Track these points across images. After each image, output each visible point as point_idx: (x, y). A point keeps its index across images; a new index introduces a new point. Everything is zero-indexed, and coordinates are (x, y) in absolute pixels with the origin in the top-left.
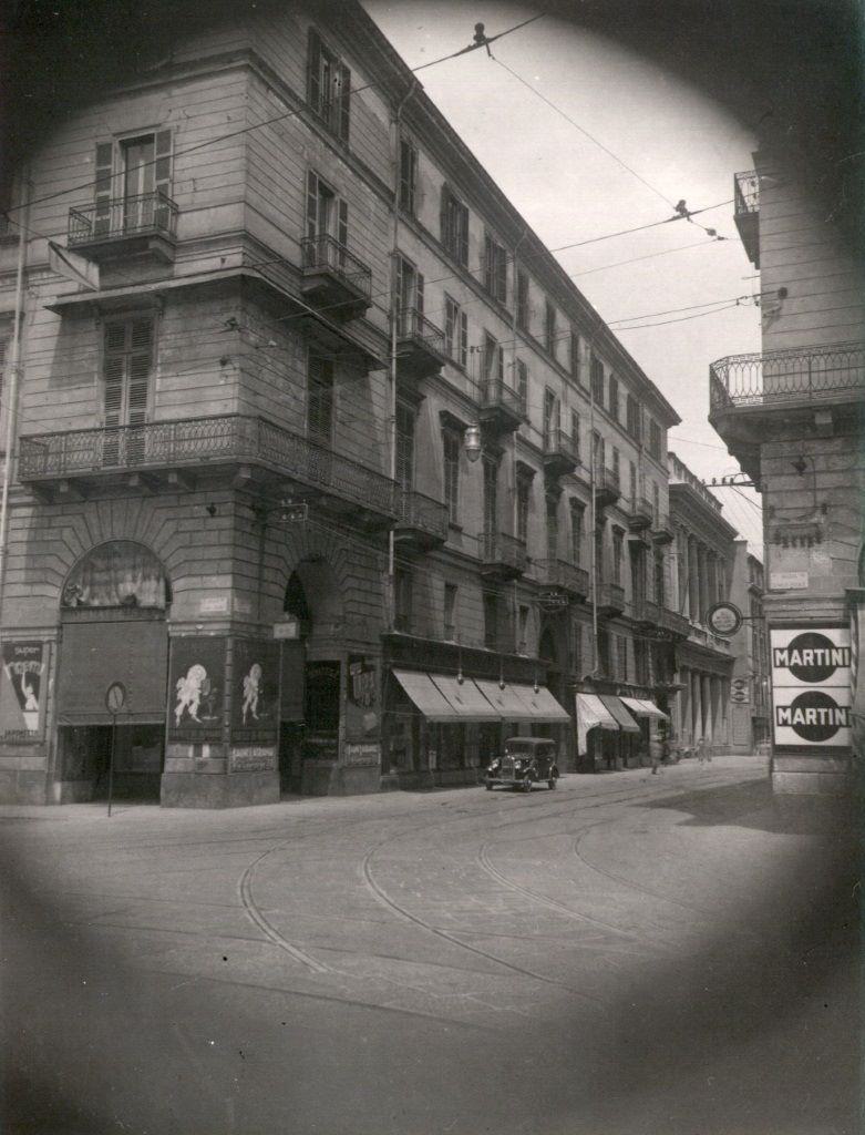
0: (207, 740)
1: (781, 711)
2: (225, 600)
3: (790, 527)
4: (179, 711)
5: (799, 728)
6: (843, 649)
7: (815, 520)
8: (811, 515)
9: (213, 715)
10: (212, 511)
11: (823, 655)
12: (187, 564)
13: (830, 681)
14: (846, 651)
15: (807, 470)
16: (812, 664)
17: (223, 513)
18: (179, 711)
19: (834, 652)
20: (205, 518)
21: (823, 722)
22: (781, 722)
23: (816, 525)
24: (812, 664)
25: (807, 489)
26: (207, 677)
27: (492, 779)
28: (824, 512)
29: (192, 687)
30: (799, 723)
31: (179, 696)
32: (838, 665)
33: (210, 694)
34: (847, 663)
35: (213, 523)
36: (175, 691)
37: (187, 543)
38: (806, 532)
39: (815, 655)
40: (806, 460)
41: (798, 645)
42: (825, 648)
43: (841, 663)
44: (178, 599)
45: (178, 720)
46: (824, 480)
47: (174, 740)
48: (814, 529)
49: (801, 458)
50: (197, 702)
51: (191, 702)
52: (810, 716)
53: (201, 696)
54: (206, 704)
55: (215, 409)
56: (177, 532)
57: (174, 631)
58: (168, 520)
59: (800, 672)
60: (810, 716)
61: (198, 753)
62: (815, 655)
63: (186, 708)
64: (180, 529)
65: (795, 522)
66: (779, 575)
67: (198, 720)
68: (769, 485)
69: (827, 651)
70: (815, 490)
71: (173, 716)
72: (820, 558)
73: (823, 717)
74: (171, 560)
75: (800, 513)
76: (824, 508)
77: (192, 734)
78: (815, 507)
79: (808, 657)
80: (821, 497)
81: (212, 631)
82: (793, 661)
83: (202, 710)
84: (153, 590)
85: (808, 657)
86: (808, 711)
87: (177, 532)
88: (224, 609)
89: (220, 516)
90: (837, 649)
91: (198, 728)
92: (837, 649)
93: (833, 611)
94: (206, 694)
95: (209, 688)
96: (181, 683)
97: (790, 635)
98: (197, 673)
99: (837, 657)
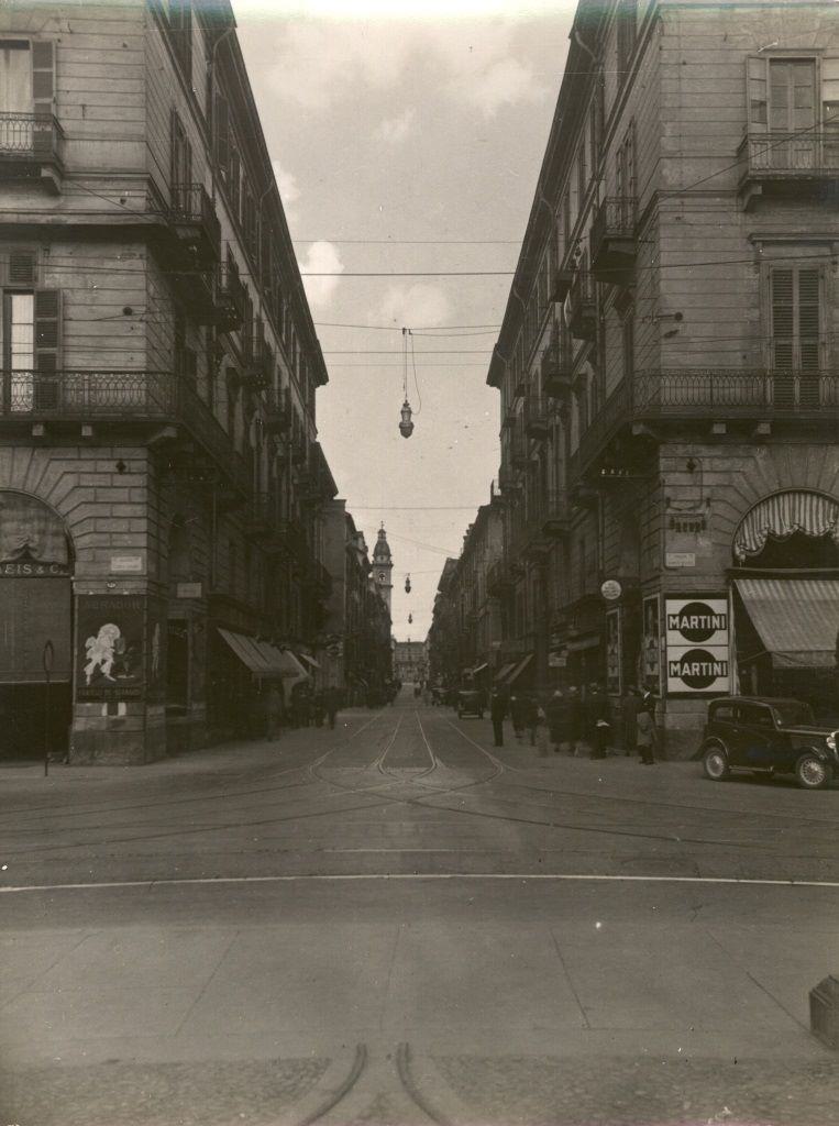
0: (125, 699)
1: (673, 665)
2: (140, 559)
3: (681, 515)
4: (89, 670)
5: (686, 679)
7: (700, 511)
8: (698, 507)
9: (128, 674)
10: (121, 469)
12: (92, 521)
14: (723, 618)
15: (696, 469)
17: (135, 471)
18: (89, 670)
20: (112, 474)
21: (704, 674)
25: (695, 485)
28: (708, 505)
29: (102, 648)
32: (716, 629)
33: (126, 652)
35: (120, 480)
36: (83, 650)
37: (91, 498)
38: (693, 521)
40: (695, 461)
41: (686, 612)
42: (707, 615)
44: (82, 556)
45: (88, 680)
46: (708, 479)
47: (83, 699)
49: (691, 459)
50: (110, 661)
51: (104, 661)
53: (115, 655)
56: (78, 487)
57: (79, 589)
58: (66, 473)
59: (686, 633)
61: (113, 710)
63: (97, 667)
64: (83, 483)
66: (672, 555)
71: (82, 675)
72: (704, 542)
75: (692, 505)
77: (101, 691)
78: (701, 500)
79: (693, 622)
80: (706, 492)
81: (126, 589)
83: (115, 670)
85: (693, 622)
87: (78, 487)
88: (139, 568)
89: (130, 473)
91: (112, 686)
92: (716, 616)
94: (121, 652)
96: (90, 642)
97: (684, 603)
98: (108, 635)
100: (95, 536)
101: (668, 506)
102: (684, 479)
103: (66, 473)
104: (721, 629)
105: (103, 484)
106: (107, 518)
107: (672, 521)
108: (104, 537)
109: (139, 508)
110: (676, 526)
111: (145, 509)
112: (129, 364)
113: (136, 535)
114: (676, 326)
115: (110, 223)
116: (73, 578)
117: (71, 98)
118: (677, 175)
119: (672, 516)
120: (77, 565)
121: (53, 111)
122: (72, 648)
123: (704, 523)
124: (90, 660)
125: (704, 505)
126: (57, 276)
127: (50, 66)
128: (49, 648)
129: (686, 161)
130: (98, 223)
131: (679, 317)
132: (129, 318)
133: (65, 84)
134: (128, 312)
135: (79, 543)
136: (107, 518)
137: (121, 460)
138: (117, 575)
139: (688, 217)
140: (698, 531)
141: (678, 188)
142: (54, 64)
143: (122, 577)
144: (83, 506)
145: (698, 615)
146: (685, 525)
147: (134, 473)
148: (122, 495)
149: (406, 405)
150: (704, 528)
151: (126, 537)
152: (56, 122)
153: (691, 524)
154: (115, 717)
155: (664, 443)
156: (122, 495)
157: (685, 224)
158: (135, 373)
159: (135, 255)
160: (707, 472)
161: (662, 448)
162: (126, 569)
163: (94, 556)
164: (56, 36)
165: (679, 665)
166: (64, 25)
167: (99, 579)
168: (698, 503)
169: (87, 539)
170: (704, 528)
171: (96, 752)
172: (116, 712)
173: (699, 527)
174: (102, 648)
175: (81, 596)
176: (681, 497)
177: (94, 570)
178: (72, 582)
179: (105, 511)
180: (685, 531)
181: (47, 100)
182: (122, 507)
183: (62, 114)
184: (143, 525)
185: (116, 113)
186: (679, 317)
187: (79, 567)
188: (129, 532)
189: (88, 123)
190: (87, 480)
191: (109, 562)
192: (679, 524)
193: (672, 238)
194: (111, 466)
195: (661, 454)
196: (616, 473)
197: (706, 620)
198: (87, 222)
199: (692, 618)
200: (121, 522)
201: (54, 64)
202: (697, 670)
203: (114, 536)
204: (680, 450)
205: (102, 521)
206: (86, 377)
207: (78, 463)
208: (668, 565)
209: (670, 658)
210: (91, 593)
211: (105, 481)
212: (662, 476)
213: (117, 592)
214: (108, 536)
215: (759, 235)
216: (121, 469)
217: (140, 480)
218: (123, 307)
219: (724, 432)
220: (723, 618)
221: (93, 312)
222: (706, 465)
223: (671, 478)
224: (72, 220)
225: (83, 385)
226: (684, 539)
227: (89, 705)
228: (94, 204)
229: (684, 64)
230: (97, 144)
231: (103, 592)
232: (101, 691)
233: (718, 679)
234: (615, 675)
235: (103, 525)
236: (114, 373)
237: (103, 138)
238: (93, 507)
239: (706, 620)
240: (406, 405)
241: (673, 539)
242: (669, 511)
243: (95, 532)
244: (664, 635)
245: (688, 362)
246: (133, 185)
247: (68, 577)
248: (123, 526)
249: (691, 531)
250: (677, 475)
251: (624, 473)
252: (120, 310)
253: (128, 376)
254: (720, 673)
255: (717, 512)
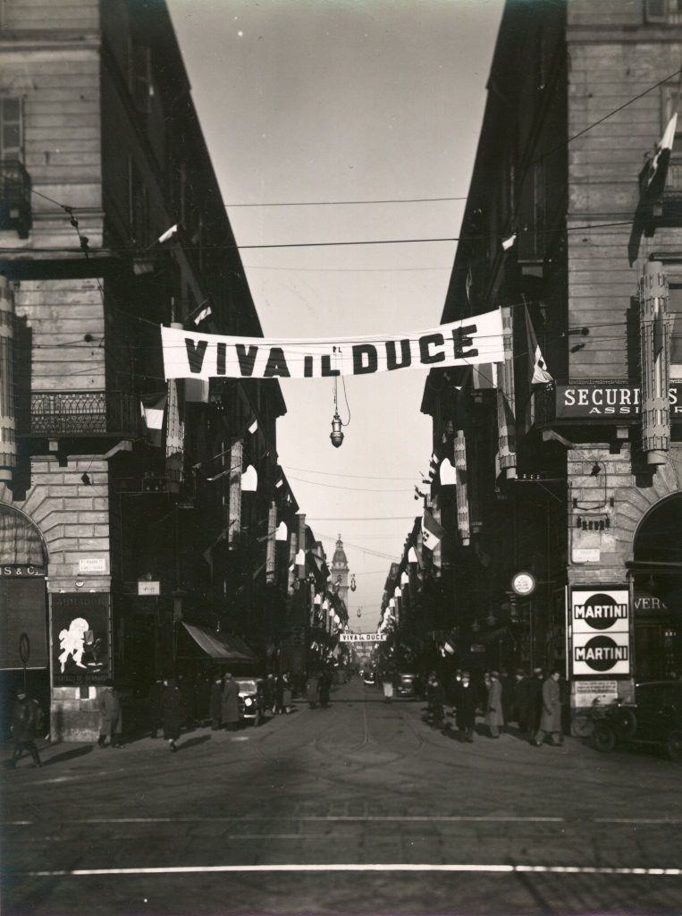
0: (93, 683)
1: (578, 650)
2: (104, 560)
3: (587, 515)
4: (63, 658)
5: (590, 663)
6: (622, 605)
10: (86, 481)
11: (609, 652)
13: (614, 628)
14: (624, 607)
15: (600, 472)
16: (600, 616)
18: (63, 658)
19: (616, 607)
20: (79, 485)
22: (578, 658)
23: (606, 514)
24: (600, 616)
25: (600, 488)
26: (89, 629)
27: (411, 799)
28: (612, 505)
29: (74, 638)
30: (590, 617)
31: (62, 646)
32: (618, 617)
33: (94, 643)
34: (624, 615)
36: (57, 642)
37: (61, 508)
38: (598, 519)
39: (603, 610)
40: (600, 465)
41: (591, 603)
43: (620, 615)
44: (55, 559)
45: (63, 670)
47: (58, 684)
48: (605, 517)
49: (596, 463)
50: (81, 651)
51: (75, 651)
52: (598, 653)
53: (85, 646)
54: (91, 653)
55: (81, 383)
56: (49, 497)
57: (53, 588)
58: (38, 485)
59: (590, 621)
60: (598, 653)
61: (85, 694)
62: (603, 610)
63: (70, 656)
65: (591, 511)
66: (579, 551)
67: (83, 666)
68: (573, 483)
69: (611, 607)
70: (606, 488)
71: (57, 664)
72: (608, 539)
73: (606, 611)
74: (44, 523)
75: (596, 505)
76: (612, 502)
77: (73, 676)
78: (605, 501)
79: (597, 611)
80: (610, 493)
81: (93, 587)
82: (588, 656)
83: (85, 659)
84: (26, 550)
85: (597, 611)
86: (597, 650)
87: (49, 497)
89: (93, 485)
90: (618, 605)
92: (618, 605)
93: (619, 575)
94: (90, 643)
95: (92, 637)
96: (63, 634)
98: (79, 627)
99: (618, 611)
100: (65, 540)
101: (576, 506)
102: (591, 481)
103: (38, 485)
104: (622, 617)
105: (70, 495)
106: (75, 524)
107: (579, 520)
108: (74, 541)
109: (102, 515)
110: (582, 525)
111: (108, 516)
112: (91, 387)
113: (99, 540)
114: (583, 340)
115: (70, 258)
116: (46, 578)
117: (37, 147)
118: (585, 200)
119: (579, 515)
120: (50, 567)
121: (21, 160)
122: (48, 640)
123: (608, 520)
124: (64, 650)
125: (608, 504)
126: (26, 308)
127: (18, 119)
128: (25, 640)
129: (592, 186)
130: (62, 258)
131: (585, 332)
132: (90, 344)
133: (30, 134)
134: (88, 338)
135: (51, 548)
136: (75, 524)
137: (85, 473)
138: (84, 575)
139: (595, 239)
140: (602, 529)
141: (584, 212)
142: (21, 117)
143: (89, 577)
144: (53, 514)
145: (602, 605)
146: (591, 523)
147: (97, 485)
148: (87, 504)
149: (337, 417)
150: (608, 526)
151: (91, 541)
152: (22, 169)
153: (596, 523)
154: (86, 700)
155: (571, 448)
156: (87, 504)
157: (592, 246)
158: (94, 393)
159: (93, 287)
160: (611, 475)
161: (570, 452)
162: (92, 570)
163: (64, 559)
164: (24, 92)
165: (584, 650)
166: (29, 82)
167: (70, 578)
168: (602, 504)
169: (57, 544)
170: (608, 526)
171: (72, 730)
172: (88, 697)
173: (602, 525)
174: (74, 638)
175: (53, 594)
176: (587, 498)
177: (62, 571)
178: (46, 582)
179: (73, 518)
180: (591, 529)
181: (15, 150)
182: (88, 514)
183: (28, 162)
184: (105, 530)
185: (76, 159)
186: (585, 332)
187: (52, 569)
188: (94, 537)
189: (51, 168)
190: (57, 491)
191: (78, 564)
192: (585, 523)
193: (579, 258)
194: (77, 479)
195: (569, 460)
196: (528, 478)
197: (609, 610)
198: (51, 258)
199: (596, 607)
200: (87, 527)
201: (21, 117)
202: (600, 654)
203: (81, 540)
204: (586, 455)
205: (70, 528)
206: (52, 398)
207: (49, 476)
208: (574, 560)
209: (575, 645)
210: (63, 591)
211: (72, 491)
212: (569, 479)
213: (84, 590)
214: (76, 540)
215: (660, 254)
216: (86, 481)
217: (104, 490)
218: (84, 335)
219: (627, 437)
220: (624, 607)
221: (58, 339)
222: (610, 469)
223: (576, 481)
224: (39, 256)
225: (49, 404)
226: (590, 537)
227: (64, 689)
228: (61, 240)
229: (591, 96)
230: (59, 187)
231: (72, 590)
232: (73, 676)
233: (619, 663)
234: (527, 659)
235: (71, 531)
236: (76, 393)
237: (64, 181)
238: (63, 514)
239: (609, 610)
240: (337, 417)
241: (580, 536)
242: (576, 511)
243: (65, 538)
244: (570, 623)
245: (594, 374)
246: (92, 222)
247: (43, 577)
248: (88, 532)
249: (596, 529)
250: (584, 478)
251: (535, 477)
252: (82, 337)
253: (88, 396)
254: (621, 657)
255: (619, 511)
